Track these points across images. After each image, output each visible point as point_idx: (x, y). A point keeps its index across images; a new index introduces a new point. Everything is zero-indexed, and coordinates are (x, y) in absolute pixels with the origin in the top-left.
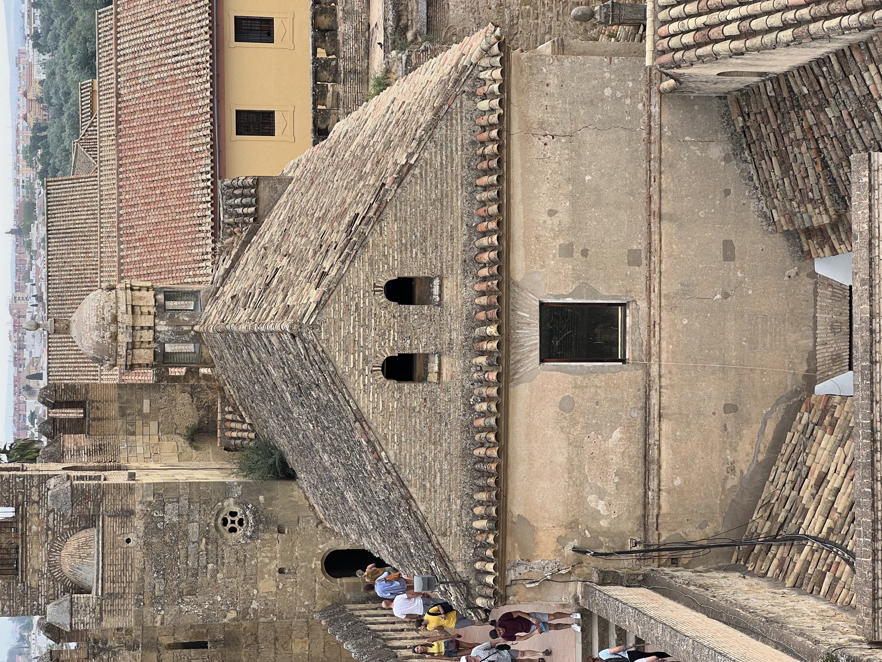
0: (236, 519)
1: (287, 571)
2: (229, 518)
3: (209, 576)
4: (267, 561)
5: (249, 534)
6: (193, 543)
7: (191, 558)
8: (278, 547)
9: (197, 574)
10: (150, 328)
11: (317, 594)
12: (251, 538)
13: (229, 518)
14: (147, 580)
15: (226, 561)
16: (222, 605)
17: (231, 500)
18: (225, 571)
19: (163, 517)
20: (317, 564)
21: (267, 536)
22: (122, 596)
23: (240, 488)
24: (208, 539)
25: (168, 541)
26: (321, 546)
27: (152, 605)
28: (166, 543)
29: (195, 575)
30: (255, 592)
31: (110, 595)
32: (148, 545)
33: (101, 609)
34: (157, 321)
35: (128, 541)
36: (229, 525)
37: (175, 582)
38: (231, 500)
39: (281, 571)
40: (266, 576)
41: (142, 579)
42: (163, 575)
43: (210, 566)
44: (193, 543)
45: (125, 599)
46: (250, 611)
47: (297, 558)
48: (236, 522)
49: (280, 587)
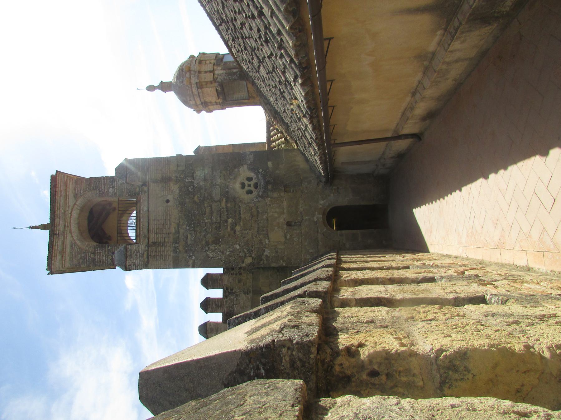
0: (252, 183)
1: (293, 224)
2: (246, 183)
3: (229, 229)
4: (276, 215)
5: (261, 193)
6: (217, 202)
7: (215, 214)
8: (285, 203)
9: (220, 226)
10: (210, 72)
11: (320, 243)
12: (262, 197)
13: (246, 183)
14: (181, 231)
15: (243, 216)
16: (240, 252)
17: (245, 167)
18: (242, 224)
19: (193, 182)
20: (318, 217)
21: (275, 195)
22: (163, 244)
23: (251, 156)
24: (227, 198)
25: (197, 201)
26: (322, 202)
27: (186, 252)
28: (195, 202)
29: (218, 228)
30: (267, 241)
31: (154, 243)
32: (182, 204)
33: (148, 254)
34: (215, 68)
35: (168, 201)
36: (247, 188)
37: (203, 234)
38: (245, 167)
39: (289, 224)
40: (276, 228)
41: (178, 232)
42: (194, 228)
43: (230, 220)
44: (217, 202)
45: (165, 247)
46: (264, 257)
47: (301, 213)
48: (252, 186)
49: (288, 237)
